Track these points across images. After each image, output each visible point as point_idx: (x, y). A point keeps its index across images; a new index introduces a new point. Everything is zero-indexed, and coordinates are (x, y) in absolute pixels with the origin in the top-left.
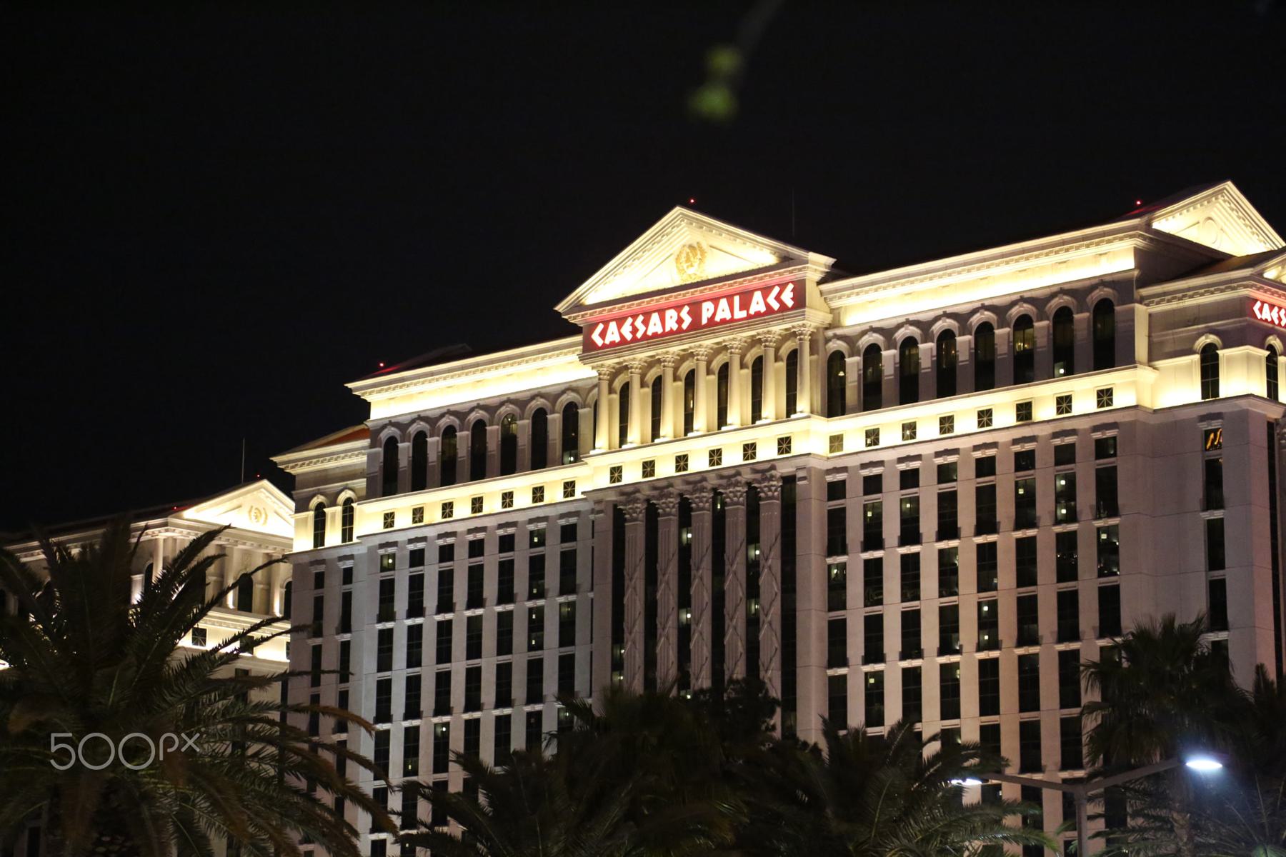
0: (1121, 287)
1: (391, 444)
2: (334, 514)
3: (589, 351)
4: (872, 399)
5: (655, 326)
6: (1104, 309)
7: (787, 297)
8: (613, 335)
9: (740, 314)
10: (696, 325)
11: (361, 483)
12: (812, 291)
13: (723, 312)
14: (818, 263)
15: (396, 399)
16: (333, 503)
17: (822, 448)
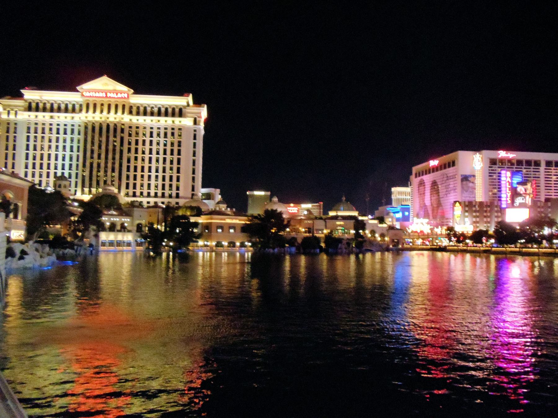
0: (185, 107)
1: (30, 104)
2: (12, 112)
3: (83, 95)
4: (138, 114)
5: (97, 95)
6: (181, 110)
7: (126, 95)
8: (88, 94)
9: (116, 97)
10: (106, 96)
11: (22, 108)
12: (130, 95)
13: (112, 95)
14: (132, 91)
15: (30, 95)
16: (12, 110)
17: (128, 120)
